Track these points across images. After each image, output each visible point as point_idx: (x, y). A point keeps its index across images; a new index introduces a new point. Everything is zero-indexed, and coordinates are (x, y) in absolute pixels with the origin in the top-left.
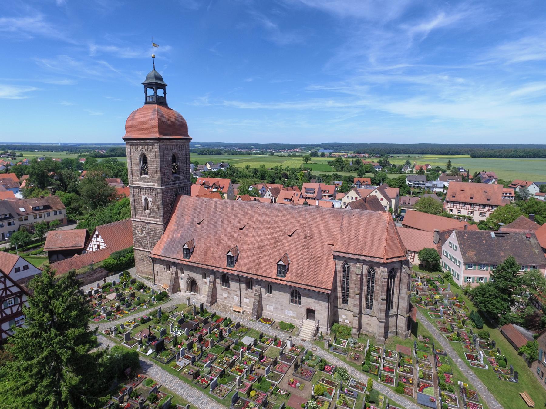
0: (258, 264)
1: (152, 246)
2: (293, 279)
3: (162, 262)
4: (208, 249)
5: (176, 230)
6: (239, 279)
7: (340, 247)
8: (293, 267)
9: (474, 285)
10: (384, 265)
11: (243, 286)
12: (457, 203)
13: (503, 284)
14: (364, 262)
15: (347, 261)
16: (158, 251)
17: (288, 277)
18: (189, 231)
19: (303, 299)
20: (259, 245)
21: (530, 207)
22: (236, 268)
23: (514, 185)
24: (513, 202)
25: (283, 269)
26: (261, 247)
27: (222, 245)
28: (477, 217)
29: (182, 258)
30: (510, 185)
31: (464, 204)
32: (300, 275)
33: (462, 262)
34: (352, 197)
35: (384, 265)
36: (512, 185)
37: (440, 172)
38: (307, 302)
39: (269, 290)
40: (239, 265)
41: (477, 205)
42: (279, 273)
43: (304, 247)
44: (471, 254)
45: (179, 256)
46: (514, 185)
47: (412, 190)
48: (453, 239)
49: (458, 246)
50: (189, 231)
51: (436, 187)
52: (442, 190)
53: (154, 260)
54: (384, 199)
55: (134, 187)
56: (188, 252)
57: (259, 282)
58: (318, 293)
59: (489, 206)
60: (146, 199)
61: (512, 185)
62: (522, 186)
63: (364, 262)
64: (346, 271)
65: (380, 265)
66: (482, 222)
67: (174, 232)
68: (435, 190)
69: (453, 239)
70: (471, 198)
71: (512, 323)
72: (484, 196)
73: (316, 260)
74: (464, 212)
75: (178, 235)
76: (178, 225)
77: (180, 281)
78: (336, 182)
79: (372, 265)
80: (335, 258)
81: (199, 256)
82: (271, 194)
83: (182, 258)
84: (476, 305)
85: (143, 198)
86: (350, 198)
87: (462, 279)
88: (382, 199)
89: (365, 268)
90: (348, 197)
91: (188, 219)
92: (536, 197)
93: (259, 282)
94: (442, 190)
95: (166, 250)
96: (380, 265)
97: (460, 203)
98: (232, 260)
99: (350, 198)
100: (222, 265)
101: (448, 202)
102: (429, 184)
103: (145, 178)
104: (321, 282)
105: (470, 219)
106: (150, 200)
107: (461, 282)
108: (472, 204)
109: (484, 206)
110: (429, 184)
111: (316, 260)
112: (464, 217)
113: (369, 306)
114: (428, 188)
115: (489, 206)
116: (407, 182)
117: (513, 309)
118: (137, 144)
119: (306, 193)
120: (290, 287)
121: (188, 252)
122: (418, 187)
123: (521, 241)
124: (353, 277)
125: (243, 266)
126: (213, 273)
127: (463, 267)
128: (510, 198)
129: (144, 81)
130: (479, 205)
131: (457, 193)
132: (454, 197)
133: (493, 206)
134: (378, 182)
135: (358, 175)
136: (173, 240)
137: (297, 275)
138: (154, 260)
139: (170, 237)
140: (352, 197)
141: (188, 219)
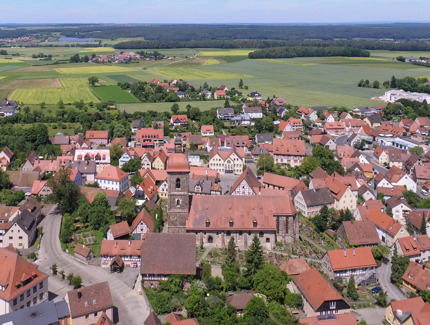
0: (243, 224)
1: (184, 224)
2: (260, 227)
3: (193, 231)
4: (217, 221)
5: (196, 214)
6: (236, 232)
7: (275, 212)
8: (259, 223)
9: (313, 216)
10: (291, 216)
11: (238, 234)
12: (280, 155)
13: (324, 215)
14: (285, 216)
15: (278, 217)
16: (190, 225)
17: (258, 227)
18: (203, 213)
19: (265, 235)
20: (241, 215)
21: (319, 152)
22: (234, 227)
23: (300, 112)
24: (302, 130)
25: (255, 224)
26: (242, 216)
27: (223, 218)
28: (293, 164)
29: (205, 227)
30: (297, 112)
31: (284, 155)
32: (262, 225)
33: (306, 206)
34: (217, 159)
35: (291, 216)
36: (299, 112)
37: (237, 95)
38: (266, 236)
39: (250, 234)
40: (235, 226)
41: (292, 155)
42: (254, 225)
43: (261, 213)
44: (308, 201)
45: (204, 227)
46: (300, 112)
47: (226, 124)
48: (300, 194)
49: (303, 198)
50: (203, 213)
53: (188, 231)
56: (208, 224)
57: (245, 231)
58: (271, 231)
59: (299, 156)
61: (299, 112)
62: (306, 114)
63: (285, 216)
64: (278, 221)
65: (290, 216)
66: (297, 167)
67: (194, 215)
68: (243, 122)
69: (300, 194)
70: (288, 151)
71: (328, 228)
72: (295, 149)
73: (267, 218)
74: (285, 161)
75: (198, 216)
76: (195, 211)
77: (204, 238)
78: (159, 122)
79: (287, 217)
80: (274, 216)
81: (214, 225)
82: (148, 160)
83: (205, 227)
84: (315, 224)
86: (215, 160)
87: (306, 213)
88: (238, 159)
89: (285, 218)
90: (214, 159)
91: (200, 207)
92: (316, 123)
93: (245, 231)
94: (249, 122)
95: (194, 225)
96: (290, 216)
97: (282, 155)
98: (232, 224)
99: (215, 160)
100: (227, 227)
101: (274, 154)
102: (238, 118)
104: (271, 227)
105: (289, 165)
107: (306, 215)
108: (289, 155)
109: (296, 156)
110: (238, 118)
111: (267, 218)
112: (286, 164)
113: (287, 232)
114: (237, 121)
115: (299, 156)
116: (218, 116)
117: (328, 223)
119: (168, 153)
120: (259, 231)
121: (208, 224)
122: (228, 119)
123: (325, 191)
124: (281, 222)
125: (237, 226)
126: (223, 231)
127: (306, 208)
128: (300, 127)
130: (293, 156)
131: (279, 148)
132: (277, 150)
133: (301, 156)
134: (192, 117)
135: (172, 110)
137: (261, 225)
138: (188, 231)
139: (194, 218)
140: (217, 159)
141: (200, 207)
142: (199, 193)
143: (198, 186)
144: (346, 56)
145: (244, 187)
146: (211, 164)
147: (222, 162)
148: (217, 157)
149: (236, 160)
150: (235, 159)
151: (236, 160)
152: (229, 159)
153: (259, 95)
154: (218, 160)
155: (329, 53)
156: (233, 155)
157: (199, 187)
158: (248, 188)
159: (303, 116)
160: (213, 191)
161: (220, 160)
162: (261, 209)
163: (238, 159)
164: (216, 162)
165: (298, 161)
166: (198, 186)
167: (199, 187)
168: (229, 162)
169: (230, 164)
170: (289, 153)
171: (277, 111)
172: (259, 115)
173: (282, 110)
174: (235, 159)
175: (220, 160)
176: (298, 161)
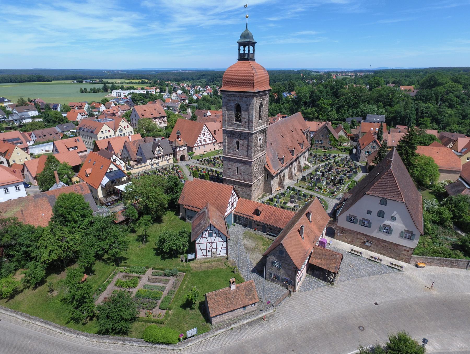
26: (292, 141)
51: (25, 119)
52: (30, 120)
54: (129, 126)
55: (255, 133)
59: (162, 117)
60: (260, 139)
68: (24, 121)
85: (259, 138)
86: (104, 132)
88: (128, 126)
94: (30, 120)
95: (275, 167)
99: (104, 132)
103: (260, 123)
106: (262, 138)
109: (160, 118)
115: (162, 117)
118: (260, 96)
128: (86, 116)
129: (238, 39)
133: (164, 117)
136: (272, 160)
140: (106, 131)
142: (160, 157)
143: (159, 147)
144: (33, 81)
145: (204, 134)
146: (101, 138)
147: (112, 133)
148: (105, 128)
149: (126, 127)
150: (125, 127)
151: (126, 127)
152: (120, 127)
153: (9, 101)
154: (108, 131)
155: (16, 79)
156: (123, 122)
157: (160, 148)
158: (208, 134)
159: (76, 108)
160: (179, 147)
161: (109, 131)
162: (296, 130)
163: (128, 126)
164: (105, 135)
165: (162, 122)
166: (159, 147)
167: (160, 148)
168: (121, 131)
169: (123, 133)
170: (154, 116)
171: (51, 107)
172: (35, 113)
173: (56, 106)
174: (125, 127)
175: (109, 131)
176: (162, 122)
